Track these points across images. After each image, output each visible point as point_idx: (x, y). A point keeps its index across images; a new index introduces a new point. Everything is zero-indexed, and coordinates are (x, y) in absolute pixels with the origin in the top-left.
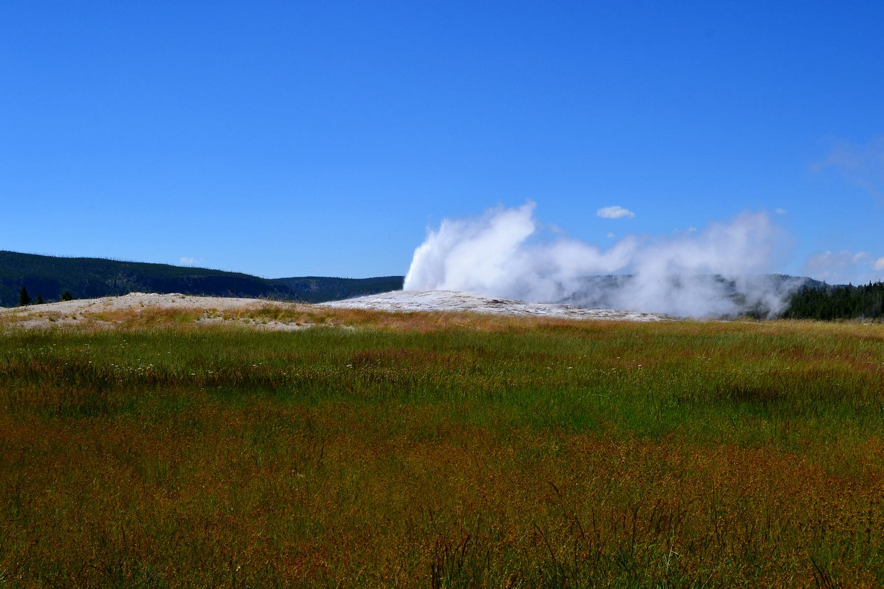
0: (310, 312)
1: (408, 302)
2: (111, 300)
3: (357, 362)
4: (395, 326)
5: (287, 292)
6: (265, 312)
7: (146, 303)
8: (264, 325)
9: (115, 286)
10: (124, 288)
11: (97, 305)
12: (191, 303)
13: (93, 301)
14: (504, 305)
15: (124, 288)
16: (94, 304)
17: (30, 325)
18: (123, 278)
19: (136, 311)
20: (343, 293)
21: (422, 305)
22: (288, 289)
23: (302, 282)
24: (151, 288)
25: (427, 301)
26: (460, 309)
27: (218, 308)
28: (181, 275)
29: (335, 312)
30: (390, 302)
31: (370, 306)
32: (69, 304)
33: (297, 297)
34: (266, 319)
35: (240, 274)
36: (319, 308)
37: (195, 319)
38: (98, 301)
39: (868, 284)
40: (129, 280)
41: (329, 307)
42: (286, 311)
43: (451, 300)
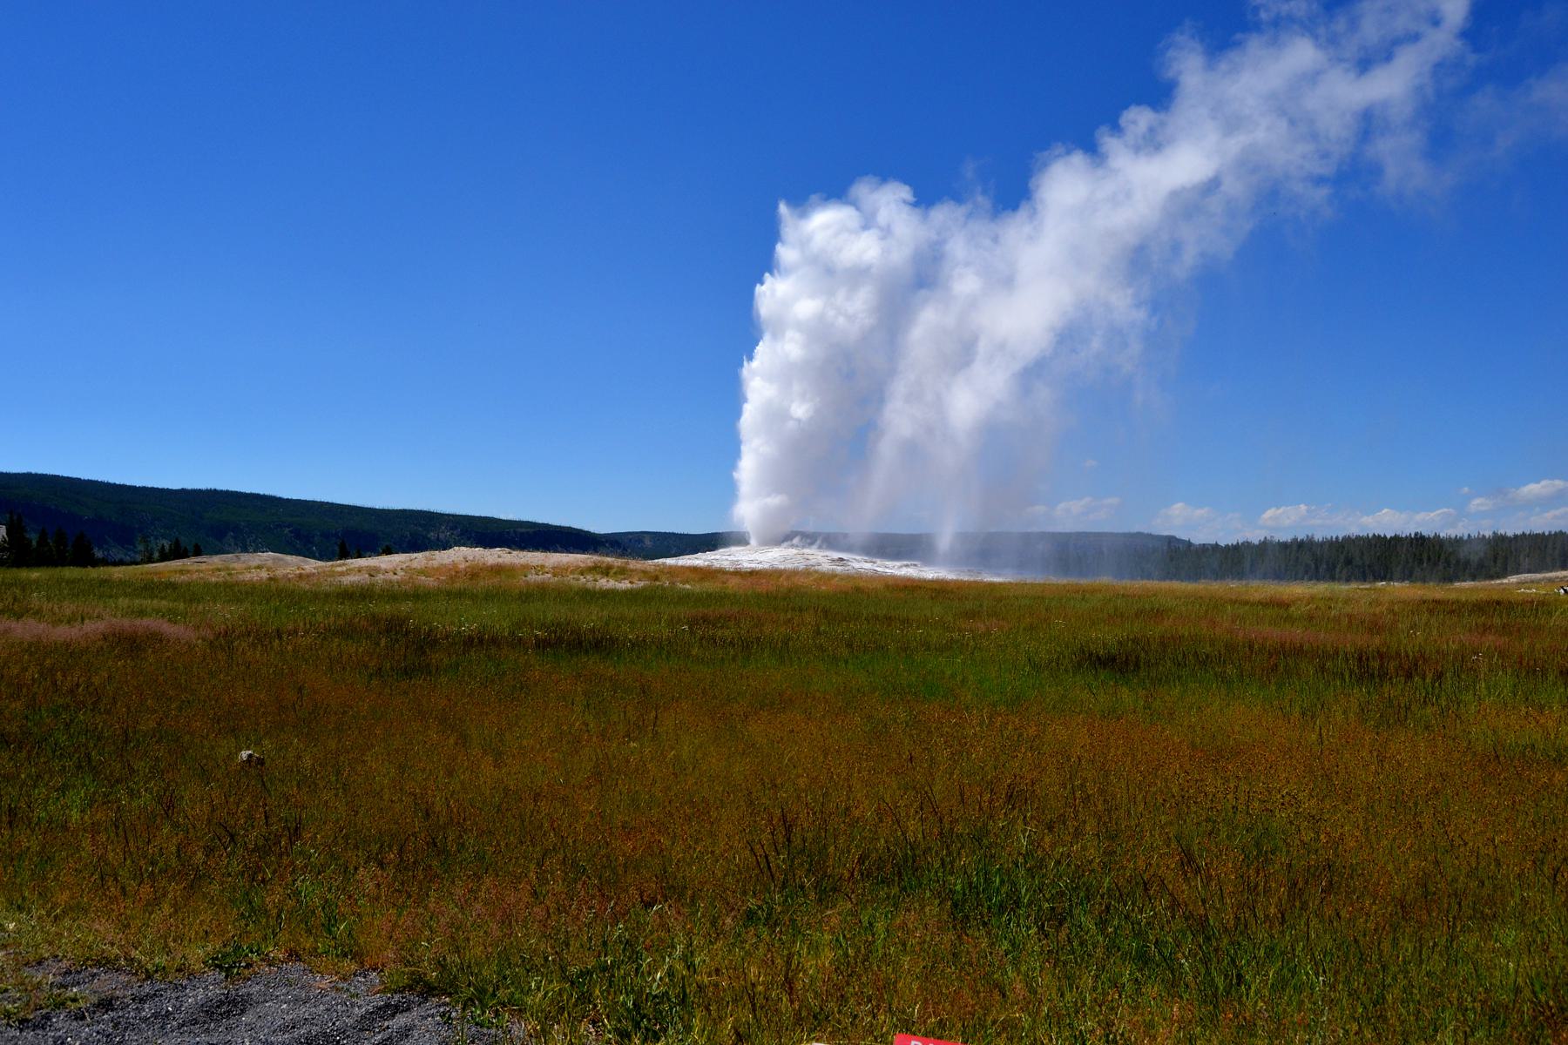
0: (643, 569)
3: (693, 622)
4: (734, 582)
6: (594, 569)
7: (471, 558)
9: (438, 539)
10: (448, 542)
11: (419, 559)
13: (415, 555)
15: (448, 542)
17: (347, 580)
19: (460, 567)
27: (547, 565)
31: (706, 563)
34: (598, 577)
38: (420, 555)
39: (1235, 543)
40: (452, 534)
41: (664, 564)
42: (618, 567)
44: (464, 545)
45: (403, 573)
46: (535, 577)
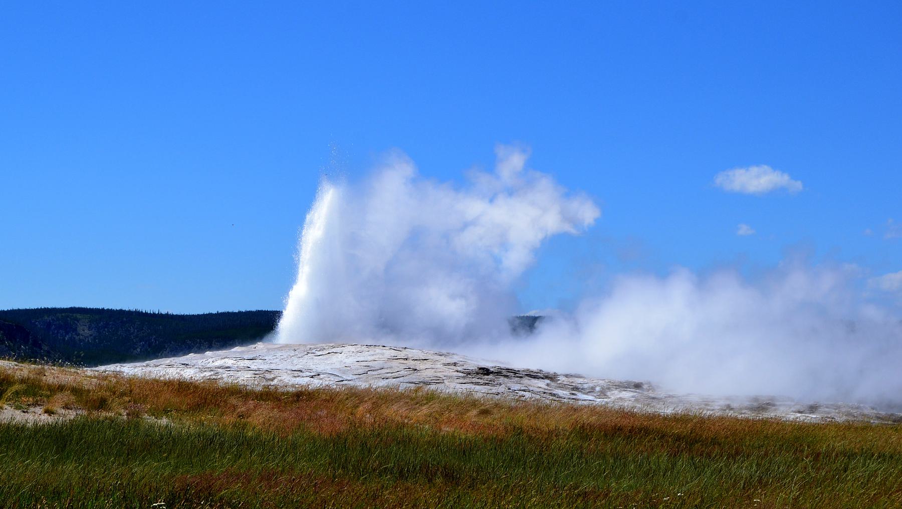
1: (290, 367)
14: (502, 380)
21: (322, 376)
25: (333, 366)
26: (405, 385)
29: (131, 386)
30: (253, 367)
31: (207, 374)
33: (48, 352)
36: (95, 377)
41: (117, 374)
42: (23, 381)
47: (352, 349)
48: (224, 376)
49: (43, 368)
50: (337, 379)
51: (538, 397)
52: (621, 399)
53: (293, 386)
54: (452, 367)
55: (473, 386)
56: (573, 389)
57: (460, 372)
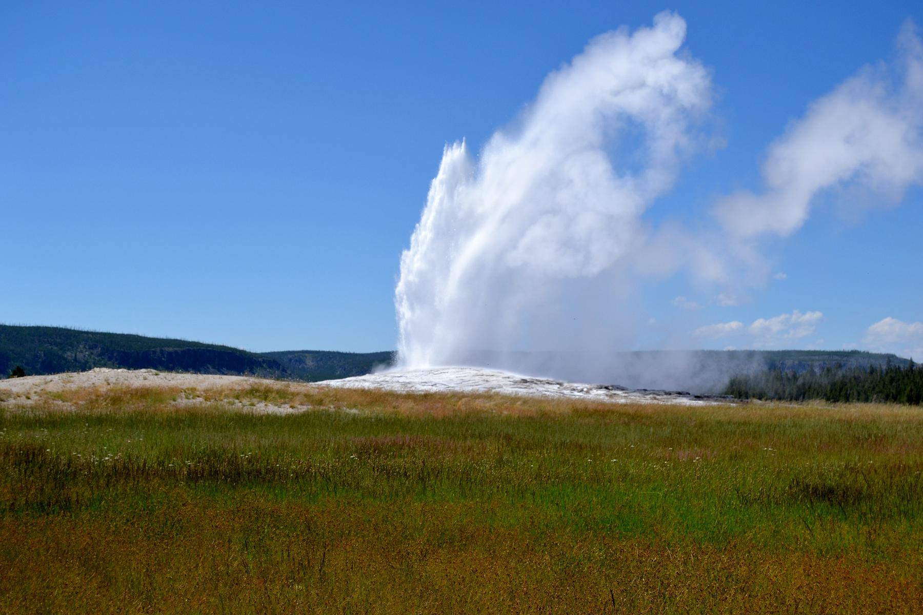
1: (421, 381)
2: (72, 377)
3: (363, 451)
4: (405, 408)
5: (278, 369)
6: (253, 392)
7: (114, 380)
8: (252, 407)
9: (75, 360)
10: (87, 362)
11: (55, 382)
12: (166, 381)
13: (49, 377)
14: (534, 385)
15: (87, 362)
16: (51, 381)
18: (84, 350)
20: (345, 370)
21: (437, 385)
22: (280, 365)
23: (295, 357)
24: (117, 362)
27: (198, 388)
28: (154, 347)
30: (400, 381)
31: (376, 385)
32: (22, 381)
33: (290, 374)
34: (255, 401)
35: (224, 348)
37: (171, 400)
38: (56, 378)
40: (92, 353)
41: (328, 386)
42: (278, 392)
43: (471, 379)
44: (105, 366)
45: (37, 398)
46: (185, 401)
47: (454, 370)
48: (385, 386)
49: (288, 384)
50: (446, 386)
51: (552, 394)
52: (597, 395)
53: (422, 391)
54: (507, 379)
55: (517, 389)
56: (572, 390)
57: (510, 381)
